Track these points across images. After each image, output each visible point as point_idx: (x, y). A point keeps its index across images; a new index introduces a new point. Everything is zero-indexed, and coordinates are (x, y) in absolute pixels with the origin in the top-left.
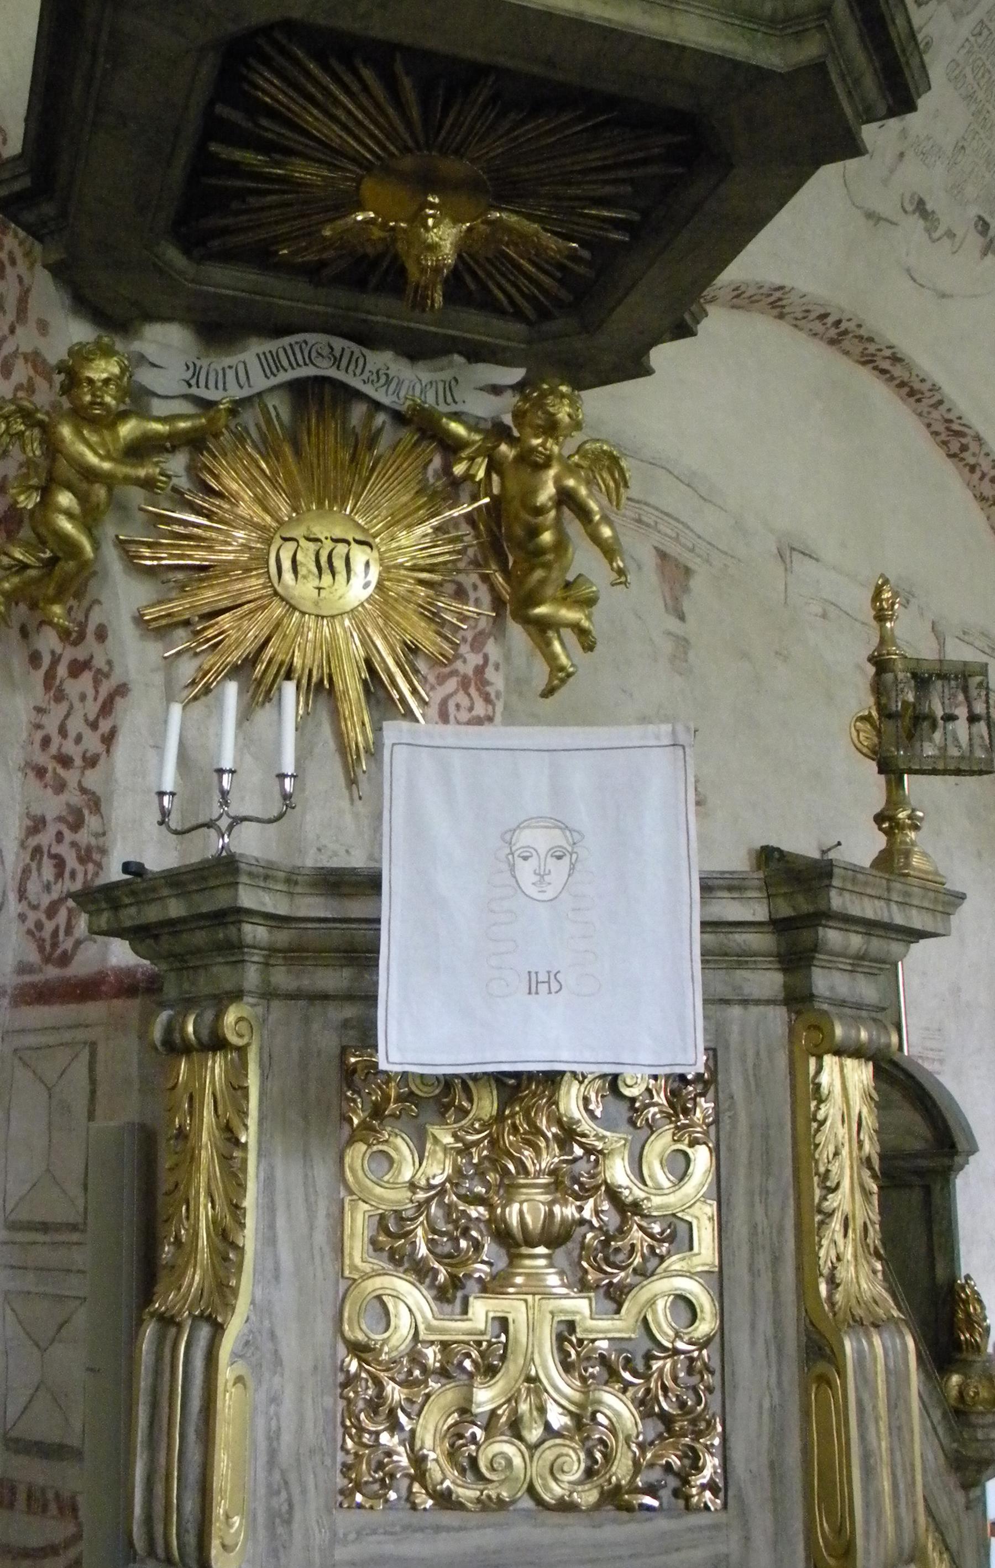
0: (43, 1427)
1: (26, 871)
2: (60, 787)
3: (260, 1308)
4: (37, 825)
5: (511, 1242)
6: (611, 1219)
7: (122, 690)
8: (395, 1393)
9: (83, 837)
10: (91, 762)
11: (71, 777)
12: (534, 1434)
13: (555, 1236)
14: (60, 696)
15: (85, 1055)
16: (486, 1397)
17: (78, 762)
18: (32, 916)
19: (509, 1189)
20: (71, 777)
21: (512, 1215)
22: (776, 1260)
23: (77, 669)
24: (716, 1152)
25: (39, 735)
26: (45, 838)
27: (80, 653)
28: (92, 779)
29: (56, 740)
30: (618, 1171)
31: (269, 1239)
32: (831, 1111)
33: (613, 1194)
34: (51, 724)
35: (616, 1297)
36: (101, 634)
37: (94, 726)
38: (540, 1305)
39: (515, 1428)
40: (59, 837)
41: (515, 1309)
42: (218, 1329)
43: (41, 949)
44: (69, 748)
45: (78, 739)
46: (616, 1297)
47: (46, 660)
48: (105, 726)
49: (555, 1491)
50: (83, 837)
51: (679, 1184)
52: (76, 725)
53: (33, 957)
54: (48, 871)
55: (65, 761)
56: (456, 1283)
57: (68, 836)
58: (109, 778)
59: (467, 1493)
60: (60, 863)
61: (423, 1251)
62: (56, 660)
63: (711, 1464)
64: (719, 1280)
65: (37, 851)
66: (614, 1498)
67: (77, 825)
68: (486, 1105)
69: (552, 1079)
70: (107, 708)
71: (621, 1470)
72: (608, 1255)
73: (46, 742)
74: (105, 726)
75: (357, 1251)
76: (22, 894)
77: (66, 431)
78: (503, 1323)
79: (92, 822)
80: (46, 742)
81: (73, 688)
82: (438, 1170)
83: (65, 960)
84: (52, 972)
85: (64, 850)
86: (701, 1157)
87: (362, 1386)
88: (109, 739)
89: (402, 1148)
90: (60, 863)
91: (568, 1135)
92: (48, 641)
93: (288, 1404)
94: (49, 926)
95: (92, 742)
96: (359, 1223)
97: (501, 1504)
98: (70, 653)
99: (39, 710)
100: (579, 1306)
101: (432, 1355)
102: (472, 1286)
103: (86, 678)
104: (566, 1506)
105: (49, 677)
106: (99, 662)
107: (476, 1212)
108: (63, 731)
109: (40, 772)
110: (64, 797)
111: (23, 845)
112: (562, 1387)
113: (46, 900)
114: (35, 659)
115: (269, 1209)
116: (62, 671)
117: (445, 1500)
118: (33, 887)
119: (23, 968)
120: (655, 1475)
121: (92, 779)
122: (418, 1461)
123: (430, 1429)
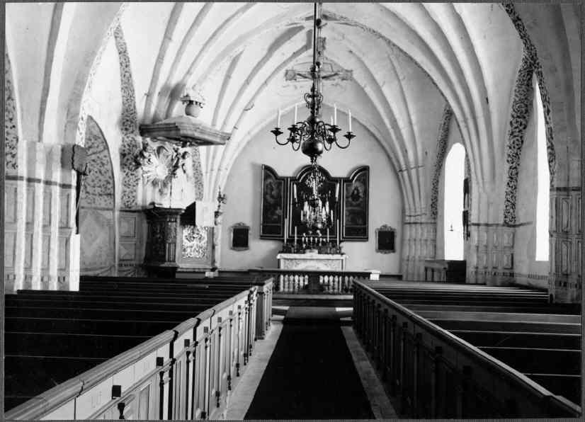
7: (139, 179)
10: (134, 186)
23: (132, 175)
26: (127, 193)
28: (135, 188)
34: (127, 179)
53: (123, 206)
60: (129, 197)
67: (132, 192)
70: (137, 180)
81: (131, 177)
88: (137, 184)
90: (129, 197)
118: (124, 198)
119: (121, 208)
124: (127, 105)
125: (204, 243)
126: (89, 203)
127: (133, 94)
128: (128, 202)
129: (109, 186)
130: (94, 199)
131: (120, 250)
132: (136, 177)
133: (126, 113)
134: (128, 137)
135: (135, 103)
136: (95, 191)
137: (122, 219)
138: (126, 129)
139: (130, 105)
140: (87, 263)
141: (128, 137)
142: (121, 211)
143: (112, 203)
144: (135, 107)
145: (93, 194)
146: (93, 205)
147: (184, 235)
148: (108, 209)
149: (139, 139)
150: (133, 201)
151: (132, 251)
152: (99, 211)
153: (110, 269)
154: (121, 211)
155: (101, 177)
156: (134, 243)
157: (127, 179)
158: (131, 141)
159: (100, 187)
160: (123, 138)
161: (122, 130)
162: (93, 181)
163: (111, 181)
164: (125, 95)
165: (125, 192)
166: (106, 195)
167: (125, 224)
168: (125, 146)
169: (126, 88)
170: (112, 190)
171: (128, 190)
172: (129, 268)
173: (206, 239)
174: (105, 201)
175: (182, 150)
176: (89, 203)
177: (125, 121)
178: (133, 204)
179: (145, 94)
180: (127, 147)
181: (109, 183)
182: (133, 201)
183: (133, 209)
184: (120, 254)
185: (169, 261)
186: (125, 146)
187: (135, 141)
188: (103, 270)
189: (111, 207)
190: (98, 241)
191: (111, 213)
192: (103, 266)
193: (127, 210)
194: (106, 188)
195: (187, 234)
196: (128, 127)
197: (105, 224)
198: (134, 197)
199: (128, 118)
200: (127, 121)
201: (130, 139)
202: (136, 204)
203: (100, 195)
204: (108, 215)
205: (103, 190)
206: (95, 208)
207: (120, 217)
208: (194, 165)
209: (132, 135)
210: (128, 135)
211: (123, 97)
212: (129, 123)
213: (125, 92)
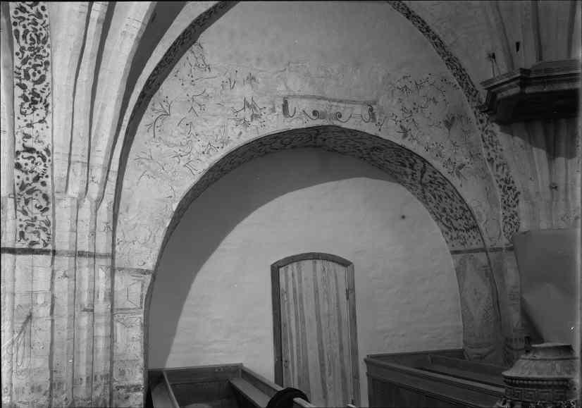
4: (506, 217)
9: (515, 220)
10: (515, 206)
11: (511, 209)
14: (507, 194)
26: (507, 220)
27: (509, 186)
28: (515, 209)
37: (514, 199)
44: (510, 203)
48: (516, 200)
50: (515, 220)
52: (511, 199)
53: (508, 242)
55: (509, 206)
65: (506, 223)
70: (516, 196)
73: (505, 202)
74: (516, 200)
85: (511, 222)
105: (504, 191)
108: (508, 201)
118: (506, 229)
121: (515, 209)
124: (464, 85)
127: (460, 66)
134: (487, 134)
135: (469, 77)
144: (472, 83)
162: (452, 211)
164: (455, 71)
174: (474, 238)
194: (466, 218)
205: (465, 221)
206: (470, 251)
211: (454, 75)
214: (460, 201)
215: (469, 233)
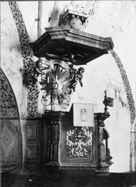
0: (33, 156)
1: (28, 108)
2: (32, 100)
3: (61, 143)
4: (29, 104)
5: (78, 138)
6: (85, 137)
7: (39, 92)
8: (70, 149)
9: (35, 105)
10: (35, 98)
11: (33, 100)
12: (79, 151)
13: (81, 138)
14: (32, 92)
15: (36, 126)
16: (77, 149)
17: (34, 98)
18: (29, 113)
19: (78, 135)
20: (33, 100)
21: (78, 136)
22: (96, 140)
23: (34, 90)
24: (92, 133)
25: (29, 95)
26: (31, 105)
27: (34, 88)
28: (36, 100)
29: (31, 96)
30: (85, 134)
31: (61, 138)
32: (100, 130)
33: (85, 135)
34: (31, 93)
35: (85, 142)
36: (37, 87)
37: (36, 95)
38: (80, 143)
39: (78, 151)
40: (32, 105)
41: (78, 143)
42: (58, 144)
43: (30, 115)
44: (33, 97)
45: (34, 96)
46: (85, 142)
47: (30, 88)
48: (37, 95)
49: (81, 156)
50: (35, 105)
51: (90, 135)
53: (29, 116)
54: (31, 108)
55: (33, 98)
56: (74, 141)
57: (33, 105)
58: (38, 100)
59: (75, 156)
60: (32, 108)
61: (72, 139)
62: (31, 88)
63: (91, 154)
64: (93, 142)
65: (29, 106)
66: (85, 156)
67: (34, 104)
68: (76, 129)
69: (81, 127)
70: (37, 94)
71: (85, 154)
72: (85, 140)
73: (30, 96)
75: (67, 139)
76: (28, 110)
77: (37, 69)
78: (77, 144)
79: (36, 104)
80: (30, 96)
81: (33, 91)
82: (73, 133)
83: (33, 116)
84: (32, 117)
85: (33, 106)
86: (91, 133)
87: (67, 149)
88: (38, 97)
89: (70, 132)
90: (32, 108)
91: (82, 131)
92: (30, 86)
93: (63, 149)
94: (31, 113)
95: (35, 97)
96: (67, 137)
97: (77, 156)
98: (33, 88)
99: (29, 93)
100: (82, 143)
101: (73, 146)
102: (75, 142)
103: (35, 91)
104: (82, 157)
105: (30, 90)
106: (36, 89)
107: (76, 136)
108: (32, 95)
109: (29, 99)
110: (32, 101)
111: (28, 105)
112: (81, 149)
113: (30, 111)
114: (29, 88)
115: (61, 136)
116: (32, 89)
117: (73, 156)
118: (29, 110)
119: (28, 117)
120: (87, 155)
121: (36, 100)
122: (72, 153)
123: (72, 151)
124: (21, 31)
125: (90, 142)
126: (4, 115)
127: (22, 19)
128: (31, 112)
129: (13, 99)
130: (6, 111)
131: (27, 151)
132: (36, 91)
133: (22, 39)
134: (27, 59)
135: (25, 27)
136: (5, 105)
137: (28, 127)
138: (25, 53)
139: (23, 30)
140: (6, 161)
141: (27, 59)
142: (27, 119)
143: (17, 114)
144: (26, 31)
145: (5, 107)
146: (6, 117)
147: (67, 137)
148: (15, 119)
149: (35, 59)
150: (35, 110)
151: (35, 151)
152: (10, 120)
153: (19, 166)
154: (27, 119)
155: (5, 92)
156: (35, 145)
157: (31, 93)
158: (30, 62)
159: (7, 101)
160: (24, 61)
161: (22, 54)
163: (12, 95)
164: (17, 22)
165: (29, 104)
166: (12, 107)
167: (30, 130)
168: (26, 67)
169: (16, 14)
170: (14, 102)
171: (31, 102)
172: (33, 165)
173: (91, 139)
174: (13, 112)
175: (76, 67)
176: (4, 115)
177: (23, 45)
178: (35, 113)
179: (36, 20)
180: (27, 67)
181: (11, 96)
182: (35, 110)
183: (35, 116)
184: (26, 154)
185: (53, 160)
186: (26, 67)
187: (32, 61)
188: (14, 167)
189: (17, 116)
190: (11, 144)
191: (18, 120)
192: (15, 163)
193: (32, 118)
194: (11, 101)
195: (70, 135)
196: (25, 50)
197: (15, 130)
198: (35, 107)
199: (24, 43)
200: (24, 45)
201: (28, 60)
202: (37, 113)
203: (9, 107)
204: (15, 123)
206: (8, 119)
207: (26, 126)
208: (128, 97)
209: (29, 57)
210: (27, 57)
211: (17, 24)
212: (26, 46)
213: (16, 20)
214: (10, 91)
215: (10, 109)
